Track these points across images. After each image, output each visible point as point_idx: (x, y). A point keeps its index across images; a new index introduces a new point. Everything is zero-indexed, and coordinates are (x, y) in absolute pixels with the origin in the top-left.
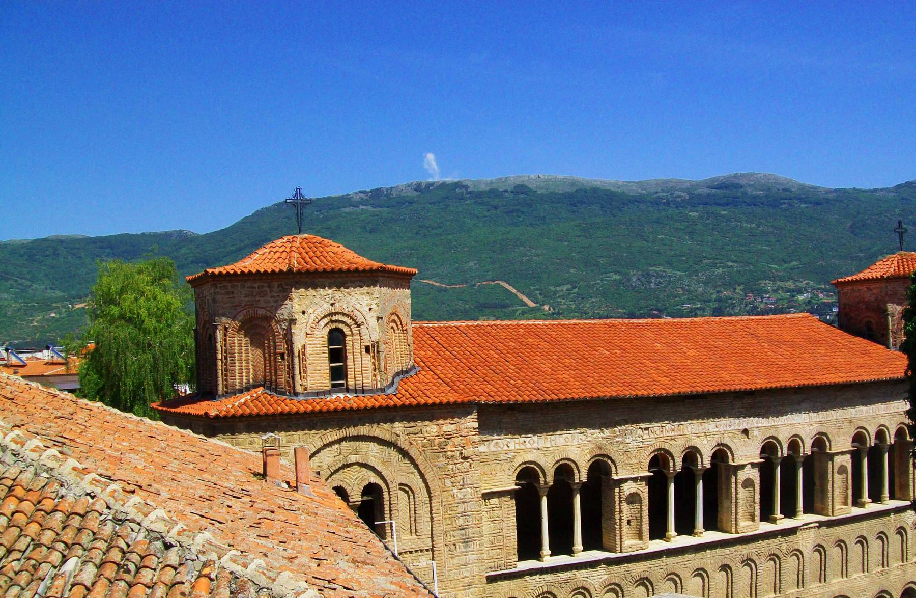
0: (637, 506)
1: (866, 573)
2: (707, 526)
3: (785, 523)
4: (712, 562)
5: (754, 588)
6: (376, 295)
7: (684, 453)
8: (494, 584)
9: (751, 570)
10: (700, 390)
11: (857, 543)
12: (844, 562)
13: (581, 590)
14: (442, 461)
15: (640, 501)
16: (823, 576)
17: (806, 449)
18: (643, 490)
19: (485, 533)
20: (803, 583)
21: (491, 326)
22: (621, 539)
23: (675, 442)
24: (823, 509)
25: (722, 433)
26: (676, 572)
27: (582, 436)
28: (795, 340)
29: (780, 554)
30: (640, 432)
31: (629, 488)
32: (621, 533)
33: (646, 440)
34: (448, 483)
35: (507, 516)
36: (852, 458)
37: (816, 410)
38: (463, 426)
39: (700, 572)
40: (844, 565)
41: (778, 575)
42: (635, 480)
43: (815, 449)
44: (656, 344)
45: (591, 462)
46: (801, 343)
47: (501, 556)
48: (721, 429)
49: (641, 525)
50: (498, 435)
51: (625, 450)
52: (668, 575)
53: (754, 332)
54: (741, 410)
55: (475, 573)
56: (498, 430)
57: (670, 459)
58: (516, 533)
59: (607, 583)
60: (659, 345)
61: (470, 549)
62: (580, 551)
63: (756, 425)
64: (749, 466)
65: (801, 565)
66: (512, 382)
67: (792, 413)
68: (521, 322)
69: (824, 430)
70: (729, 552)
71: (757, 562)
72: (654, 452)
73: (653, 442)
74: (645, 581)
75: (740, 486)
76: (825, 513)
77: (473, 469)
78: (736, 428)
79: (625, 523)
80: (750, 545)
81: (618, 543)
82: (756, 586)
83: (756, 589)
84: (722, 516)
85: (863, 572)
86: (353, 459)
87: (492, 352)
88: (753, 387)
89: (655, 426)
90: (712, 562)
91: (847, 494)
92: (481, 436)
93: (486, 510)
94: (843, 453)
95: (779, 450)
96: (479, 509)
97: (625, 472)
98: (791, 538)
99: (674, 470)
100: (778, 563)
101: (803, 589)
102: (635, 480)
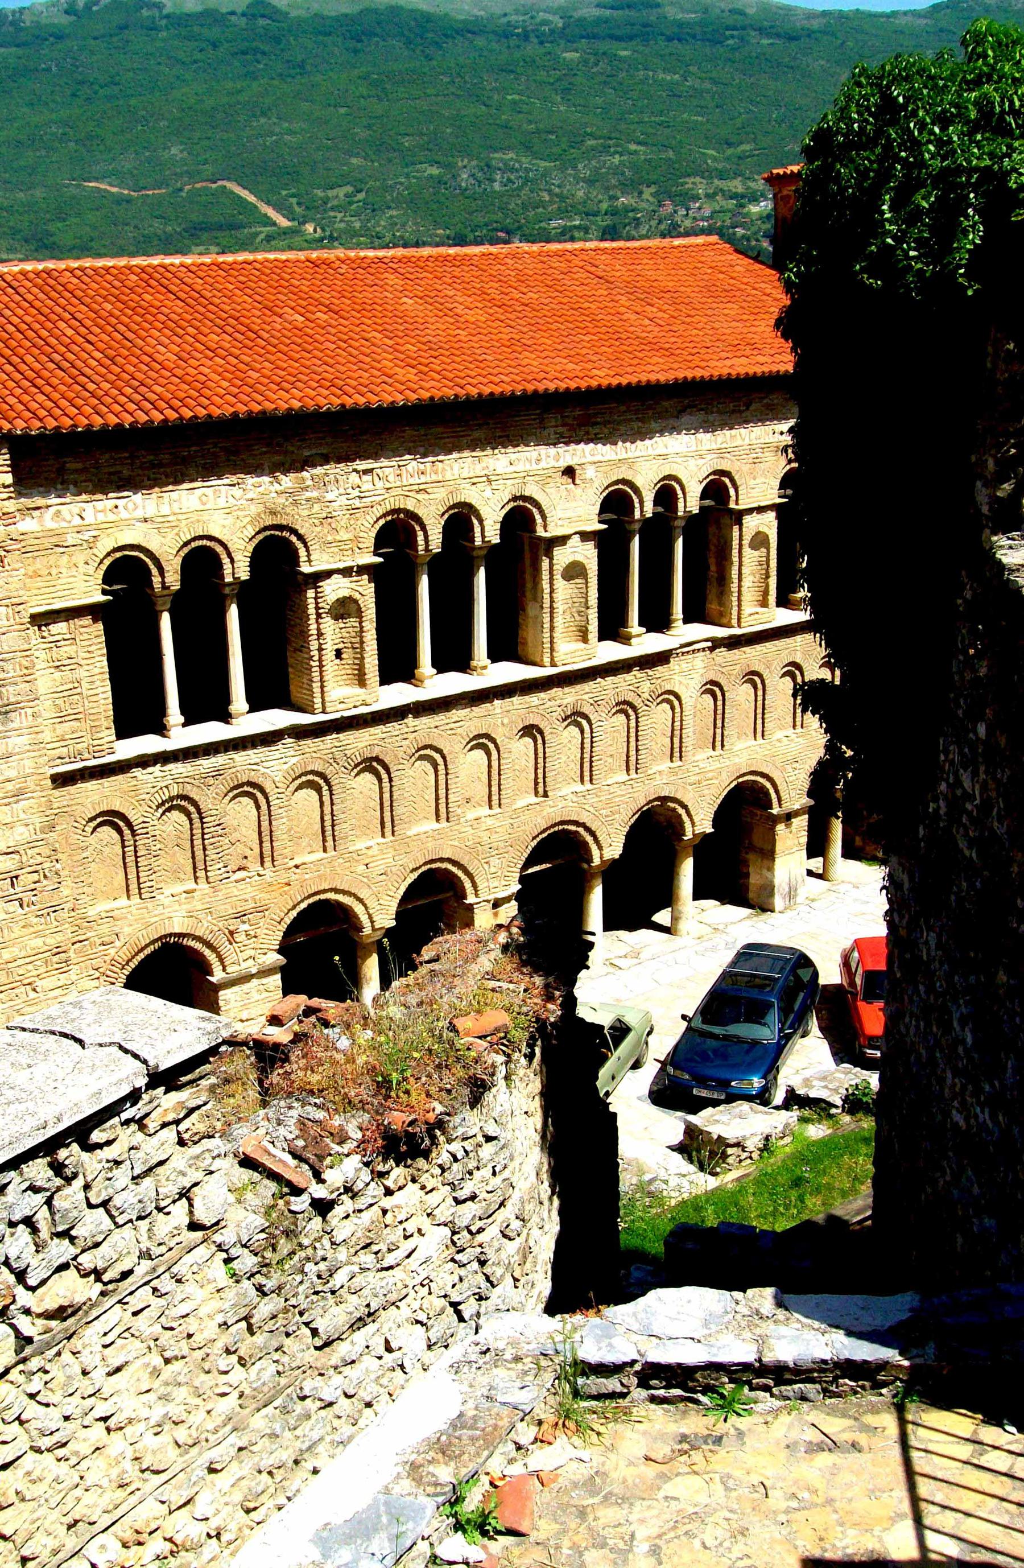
0: (353, 621)
1: (799, 729)
2: (495, 656)
3: (648, 643)
5: (587, 765)
7: (446, 516)
8: (71, 789)
9: (582, 732)
10: (474, 392)
11: (784, 675)
12: (759, 711)
13: (246, 788)
15: (359, 614)
16: (719, 738)
17: (691, 502)
18: (365, 592)
19: (42, 691)
20: (681, 752)
21: (72, 271)
22: (322, 687)
23: (426, 496)
24: (721, 614)
26: (435, 744)
27: (236, 491)
28: (683, 289)
29: (637, 702)
30: (354, 478)
31: (334, 589)
32: (322, 677)
35: (88, 655)
36: (778, 518)
37: (710, 427)
39: (483, 742)
40: (759, 716)
41: (633, 739)
42: (346, 572)
43: (708, 502)
44: (405, 300)
45: (256, 541)
46: (692, 295)
48: (520, 467)
49: (362, 658)
50: (59, 497)
52: (419, 750)
53: (601, 274)
54: (560, 429)
55: (28, 771)
56: (59, 486)
57: (417, 528)
58: (109, 688)
60: (411, 301)
61: (12, 725)
62: (242, 714)
64: (577, 538)
65: (677, 719)
66: (91, 386)
67: (661, 433)
68: (135, 261)
69: (724, 466)
70: (537, 702)
71: (592, 717)
72: (384, 515)
73: (381, 498)
74: (375, 764)
75: (558, 577)
76: (725, 621)
77: (7, 568)
79: (329, 655)
80: (578, 687)
81: (318, 695)
82: (591, 762)
83: (591, 767)
84: (528, 634)
85: (794, 727)
87: (62, 325)
88: (583, 385)
89: (386, 467)
90: (506, 721)
91: (767, 586)
92: (22, 500)
94: (761, 510)
95: (637, 505)
96: (27, 647)
97: (325, 557)
98: (660, 670)
99: (427, 550)
100: (633, 717)
101: (680, 763)
102: (346, 572)
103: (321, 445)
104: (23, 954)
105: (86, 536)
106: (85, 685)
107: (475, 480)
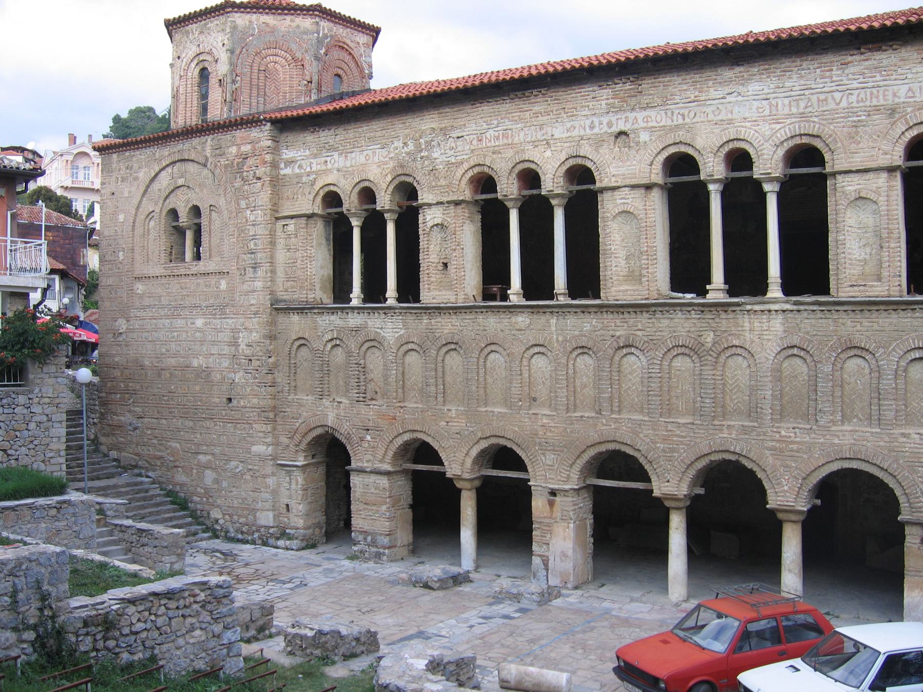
4: (560, 339)
6: (228, 30)
14: (238, 183)
23: (500, 156)
25: (577, 139)
33: (458, 154)
34: (243, 204)
38: (257, 145)
47: (295, 290)
48: (576, 133)
51: (431, 168)
59: (404, 341)
63: (645, 125)
78: (603, 131)
86: (181, 182)
93: (283, 237)
103: (432, 122)
104: (248, 405)
105: (312, 177)
106: (299, 261)
107: (536, 144)
